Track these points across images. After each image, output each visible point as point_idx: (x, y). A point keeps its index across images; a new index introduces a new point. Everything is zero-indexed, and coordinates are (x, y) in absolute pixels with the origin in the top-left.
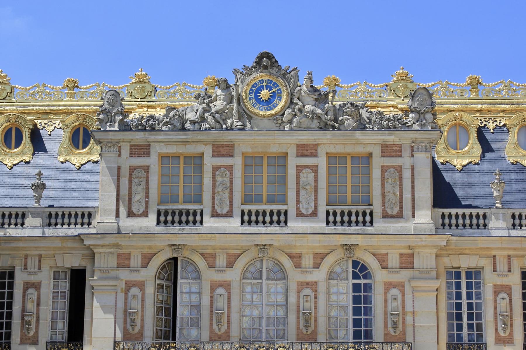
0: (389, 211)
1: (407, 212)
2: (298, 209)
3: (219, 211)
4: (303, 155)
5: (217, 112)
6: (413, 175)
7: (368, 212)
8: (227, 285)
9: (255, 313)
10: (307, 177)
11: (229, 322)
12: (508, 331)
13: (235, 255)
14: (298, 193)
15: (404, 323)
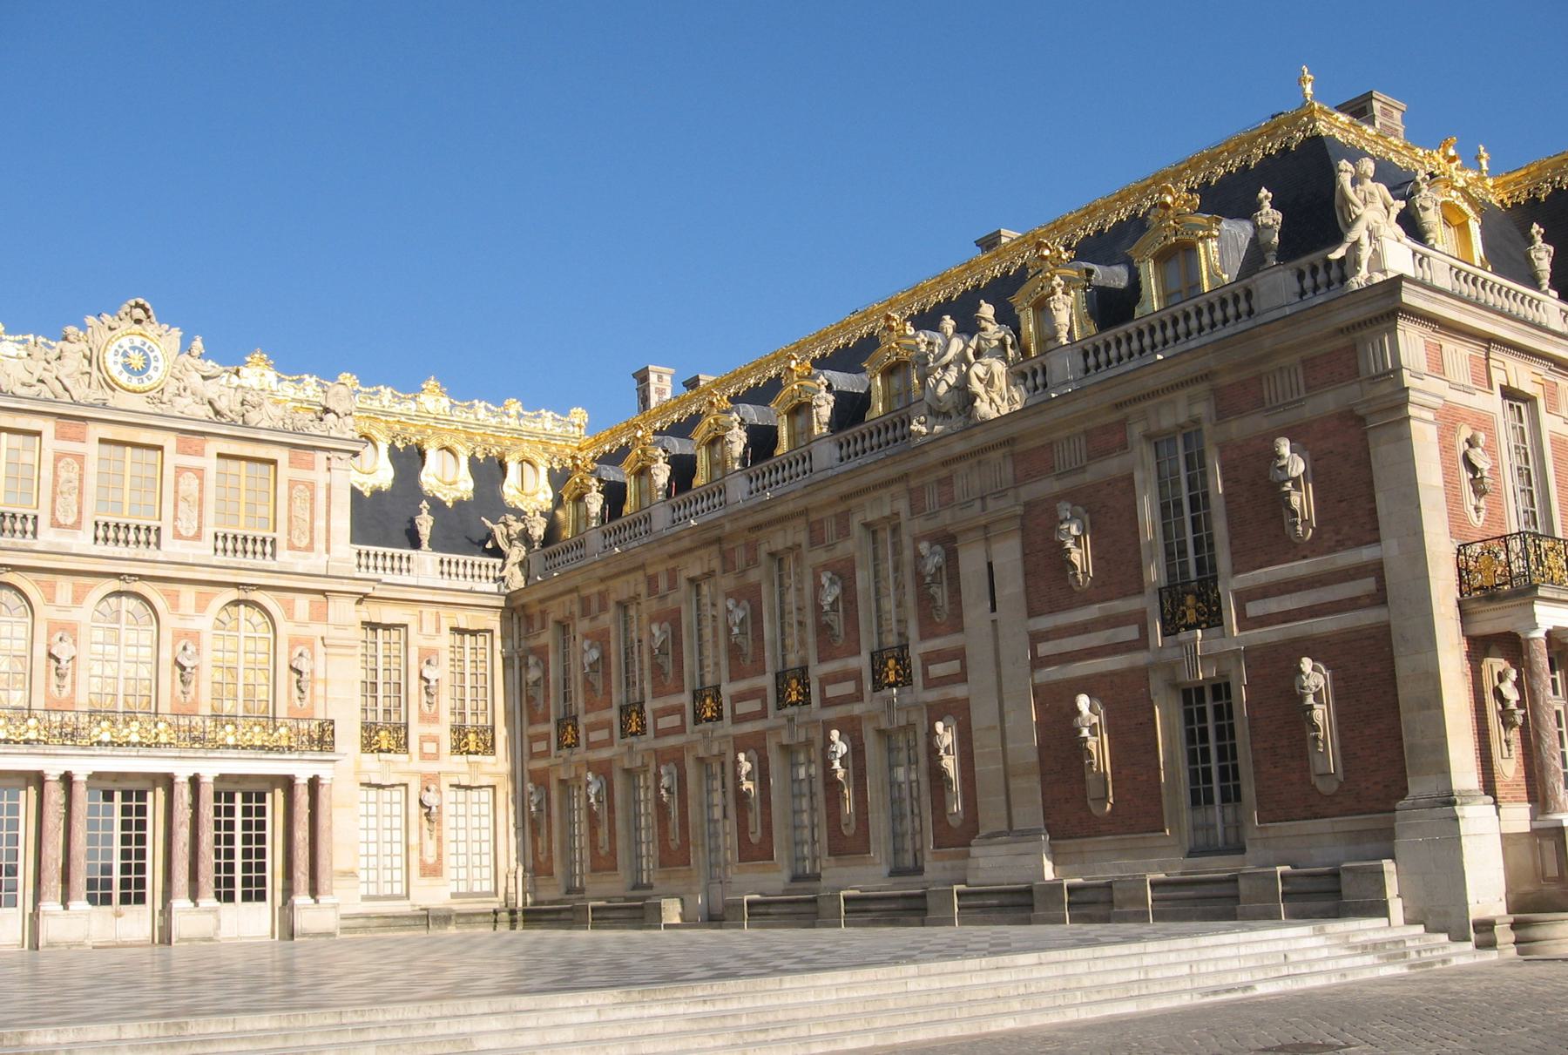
0: (296, 542)
1: (320, 545)
2: (175, 527)
3: (62, 520)
4: (184, 453)
5: (68, 376)
6: (329, 497)
7: (269, 540)
8: (68, 630)
9: (109, 671)
10: (189, 484)
11: (73, 683)
12: (434, 707)
13: (85, 586)
14: (176, 506)
15: (312, 693)
